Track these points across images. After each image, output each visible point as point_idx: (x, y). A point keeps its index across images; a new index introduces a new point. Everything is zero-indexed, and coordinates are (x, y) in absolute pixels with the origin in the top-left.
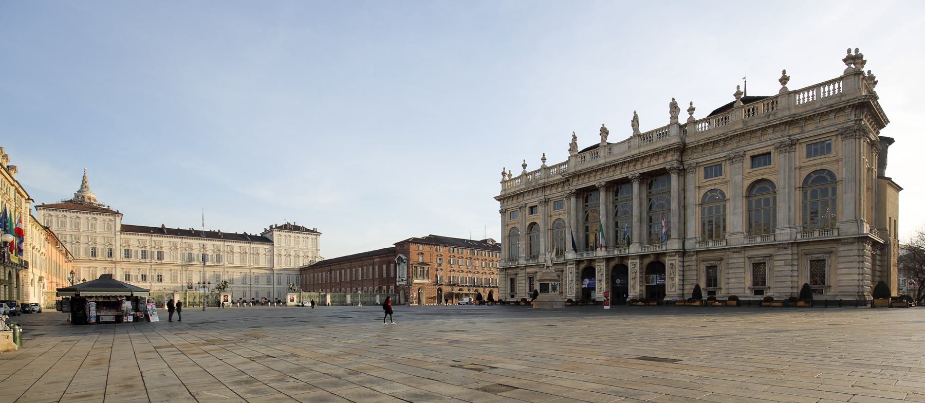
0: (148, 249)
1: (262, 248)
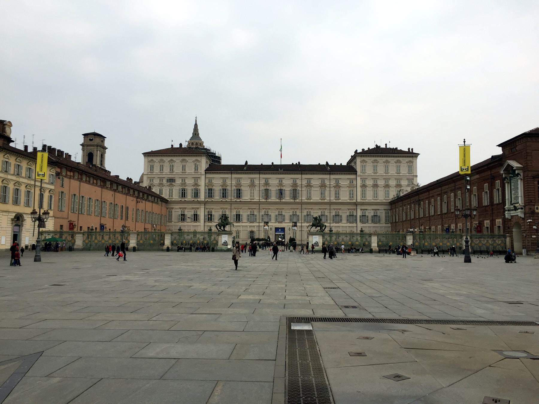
0: (229, 188)
1: (344, 179)
